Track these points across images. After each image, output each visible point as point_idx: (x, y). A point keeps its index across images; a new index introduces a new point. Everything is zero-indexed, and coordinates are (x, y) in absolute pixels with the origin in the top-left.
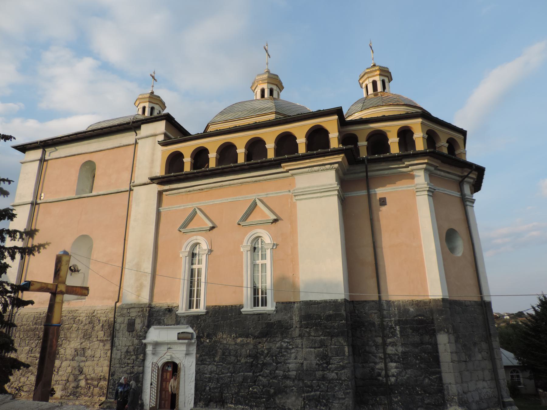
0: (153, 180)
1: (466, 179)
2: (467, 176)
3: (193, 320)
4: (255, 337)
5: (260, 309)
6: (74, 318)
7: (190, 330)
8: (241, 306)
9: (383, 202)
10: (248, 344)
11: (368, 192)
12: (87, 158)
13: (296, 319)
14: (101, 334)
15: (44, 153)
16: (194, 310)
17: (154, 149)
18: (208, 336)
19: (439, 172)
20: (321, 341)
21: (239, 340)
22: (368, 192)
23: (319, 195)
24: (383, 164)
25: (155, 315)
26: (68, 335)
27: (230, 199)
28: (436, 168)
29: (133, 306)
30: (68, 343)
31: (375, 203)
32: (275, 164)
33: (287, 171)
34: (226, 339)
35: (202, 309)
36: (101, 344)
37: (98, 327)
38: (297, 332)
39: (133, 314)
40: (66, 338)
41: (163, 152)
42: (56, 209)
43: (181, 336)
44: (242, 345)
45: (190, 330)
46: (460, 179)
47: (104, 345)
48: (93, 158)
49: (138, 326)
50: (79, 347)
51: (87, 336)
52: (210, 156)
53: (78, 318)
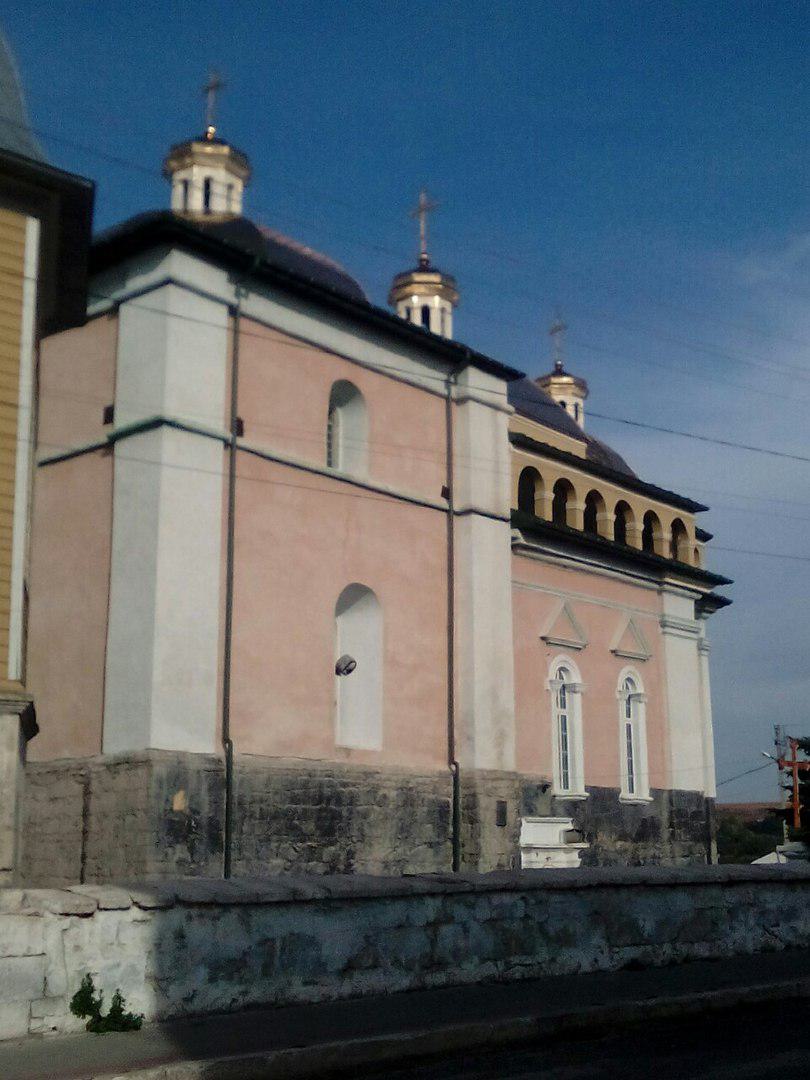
3: (572, 808)
4: (635, 841)
6: (374, 790)
10: (626, 851)
12: (344, 372)
13: (665, 815)
14: (428, 831)
21: (619, 844)
23: (683, 633)
25: (534, 797)
26: (367, 831)
29: (498, 775)
30: (368, 848)
34: (608, 842)
36: (431, 852)
39: (504, 791)
40: (362, 838)
47: (437, 853)
48: (365, 382)
49: (511, 816)
50: (391, 857)
51: (404, 832)
53: (381, 793)
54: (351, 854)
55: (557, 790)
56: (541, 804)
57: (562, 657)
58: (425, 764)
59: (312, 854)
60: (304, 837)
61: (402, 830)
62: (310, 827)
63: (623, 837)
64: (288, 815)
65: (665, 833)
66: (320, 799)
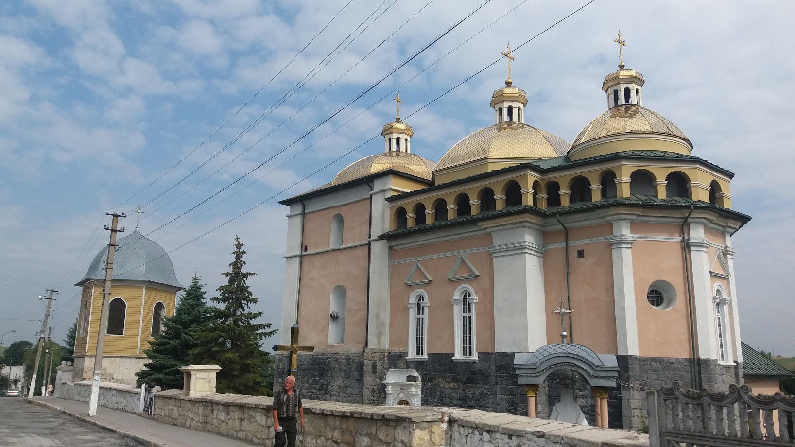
0: (380, 238)
1: (690, 220)
2: (689, 216)
3: (419, 365)
5: (467, 358)
7: (416, 374)
8: (453, 355)
9: (581, 254)
11: (567, 244)
12: (335, 212)
13: (493, 368)
15: (304, 208)
16: (420, 357)
17: (384, 206)
18: (430, 380)
19: (642, 218)
20: (510, 389)
21: (451, 385)
22: (567, 244)
23: (512, 252)
24: (579, 215)
27: (442, 255)
28: (638, 215)
31: (574, 255)
32: (474, 221)
33: (485, 229)
35: (425, 356)
37: (354, 368)
38: (493, 381)
40: (332, 377)
41: (391, 208)
42: (318, 261)
43: (411, 379)
44: (454, 389)
45: (416, 374)
46: (683, 220)
51: (347, 376)
52: (427, 212)
54: (328, 383)
55: (411, 355)
56: (401, 363)
57: (419, 290)
58: (352, 348)
59: (316, 382)
60: (314, 376)
61: (346, 374)
62: (316, 373)
63: (455, 380)
64: (310, 369)
65: (493, 381)
66: (319, 364)
